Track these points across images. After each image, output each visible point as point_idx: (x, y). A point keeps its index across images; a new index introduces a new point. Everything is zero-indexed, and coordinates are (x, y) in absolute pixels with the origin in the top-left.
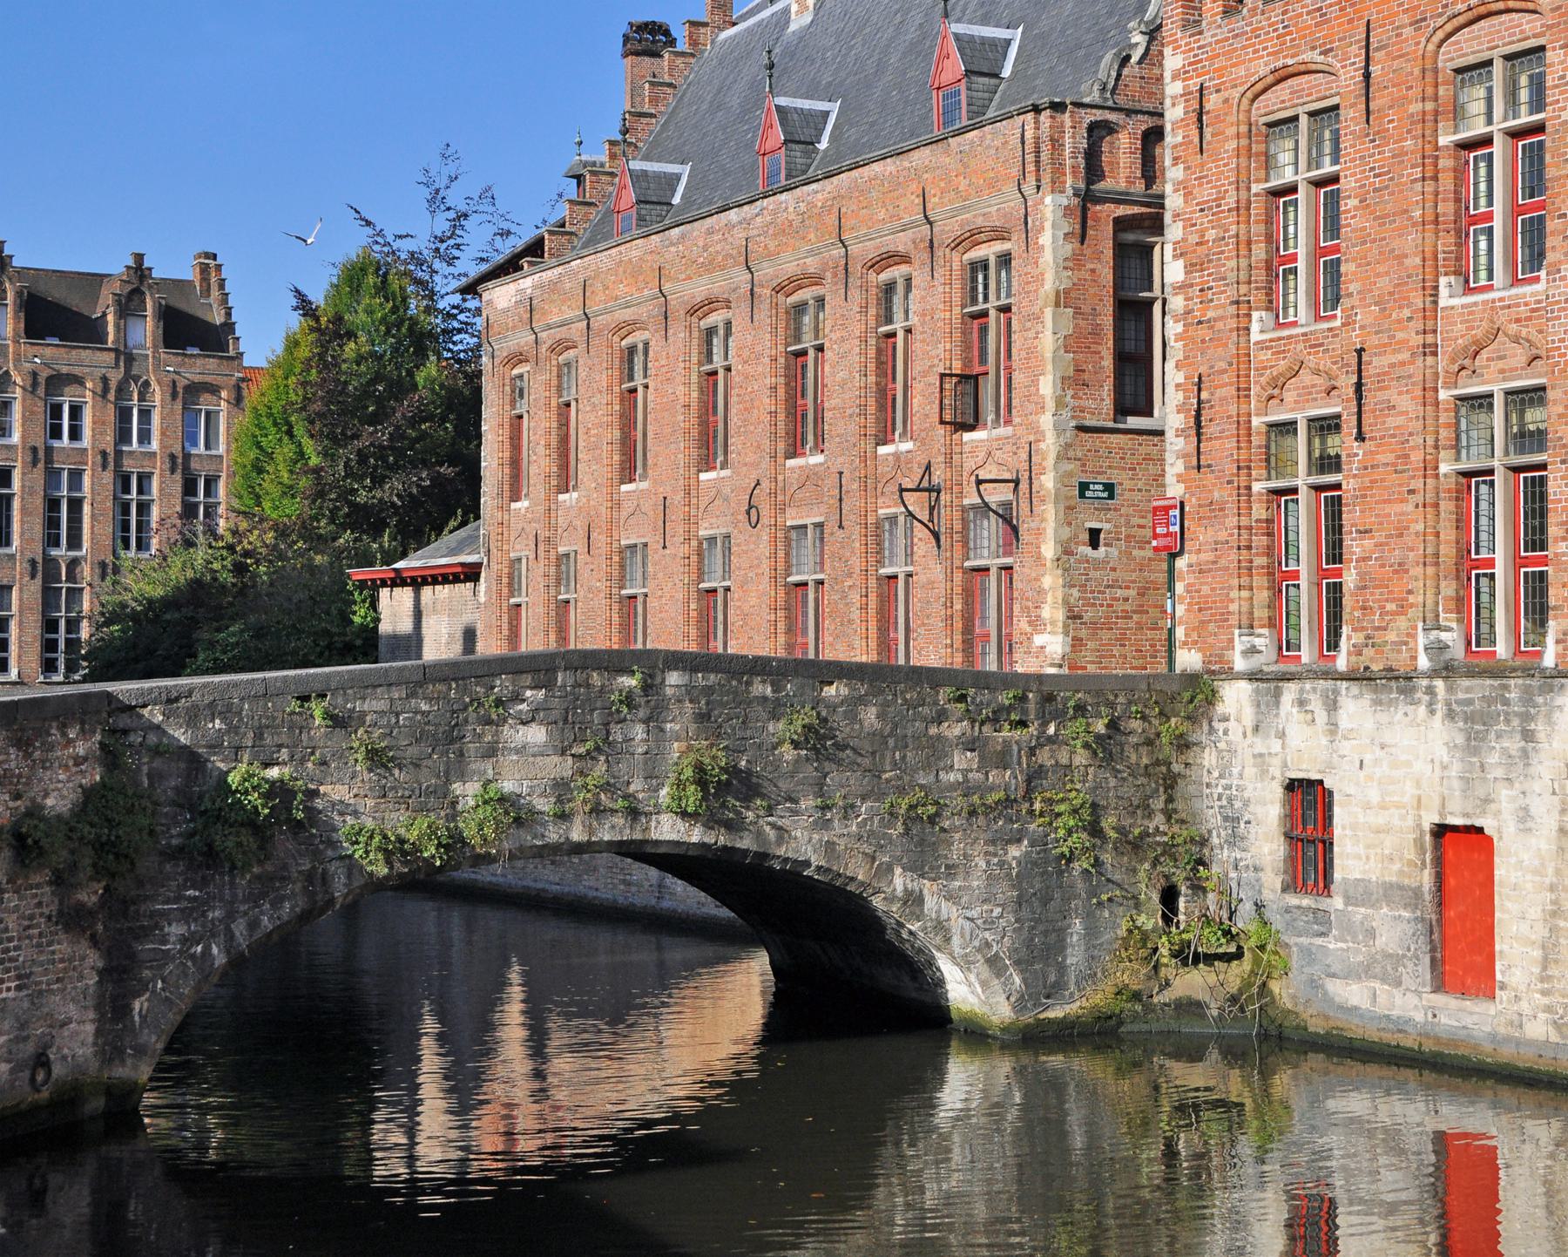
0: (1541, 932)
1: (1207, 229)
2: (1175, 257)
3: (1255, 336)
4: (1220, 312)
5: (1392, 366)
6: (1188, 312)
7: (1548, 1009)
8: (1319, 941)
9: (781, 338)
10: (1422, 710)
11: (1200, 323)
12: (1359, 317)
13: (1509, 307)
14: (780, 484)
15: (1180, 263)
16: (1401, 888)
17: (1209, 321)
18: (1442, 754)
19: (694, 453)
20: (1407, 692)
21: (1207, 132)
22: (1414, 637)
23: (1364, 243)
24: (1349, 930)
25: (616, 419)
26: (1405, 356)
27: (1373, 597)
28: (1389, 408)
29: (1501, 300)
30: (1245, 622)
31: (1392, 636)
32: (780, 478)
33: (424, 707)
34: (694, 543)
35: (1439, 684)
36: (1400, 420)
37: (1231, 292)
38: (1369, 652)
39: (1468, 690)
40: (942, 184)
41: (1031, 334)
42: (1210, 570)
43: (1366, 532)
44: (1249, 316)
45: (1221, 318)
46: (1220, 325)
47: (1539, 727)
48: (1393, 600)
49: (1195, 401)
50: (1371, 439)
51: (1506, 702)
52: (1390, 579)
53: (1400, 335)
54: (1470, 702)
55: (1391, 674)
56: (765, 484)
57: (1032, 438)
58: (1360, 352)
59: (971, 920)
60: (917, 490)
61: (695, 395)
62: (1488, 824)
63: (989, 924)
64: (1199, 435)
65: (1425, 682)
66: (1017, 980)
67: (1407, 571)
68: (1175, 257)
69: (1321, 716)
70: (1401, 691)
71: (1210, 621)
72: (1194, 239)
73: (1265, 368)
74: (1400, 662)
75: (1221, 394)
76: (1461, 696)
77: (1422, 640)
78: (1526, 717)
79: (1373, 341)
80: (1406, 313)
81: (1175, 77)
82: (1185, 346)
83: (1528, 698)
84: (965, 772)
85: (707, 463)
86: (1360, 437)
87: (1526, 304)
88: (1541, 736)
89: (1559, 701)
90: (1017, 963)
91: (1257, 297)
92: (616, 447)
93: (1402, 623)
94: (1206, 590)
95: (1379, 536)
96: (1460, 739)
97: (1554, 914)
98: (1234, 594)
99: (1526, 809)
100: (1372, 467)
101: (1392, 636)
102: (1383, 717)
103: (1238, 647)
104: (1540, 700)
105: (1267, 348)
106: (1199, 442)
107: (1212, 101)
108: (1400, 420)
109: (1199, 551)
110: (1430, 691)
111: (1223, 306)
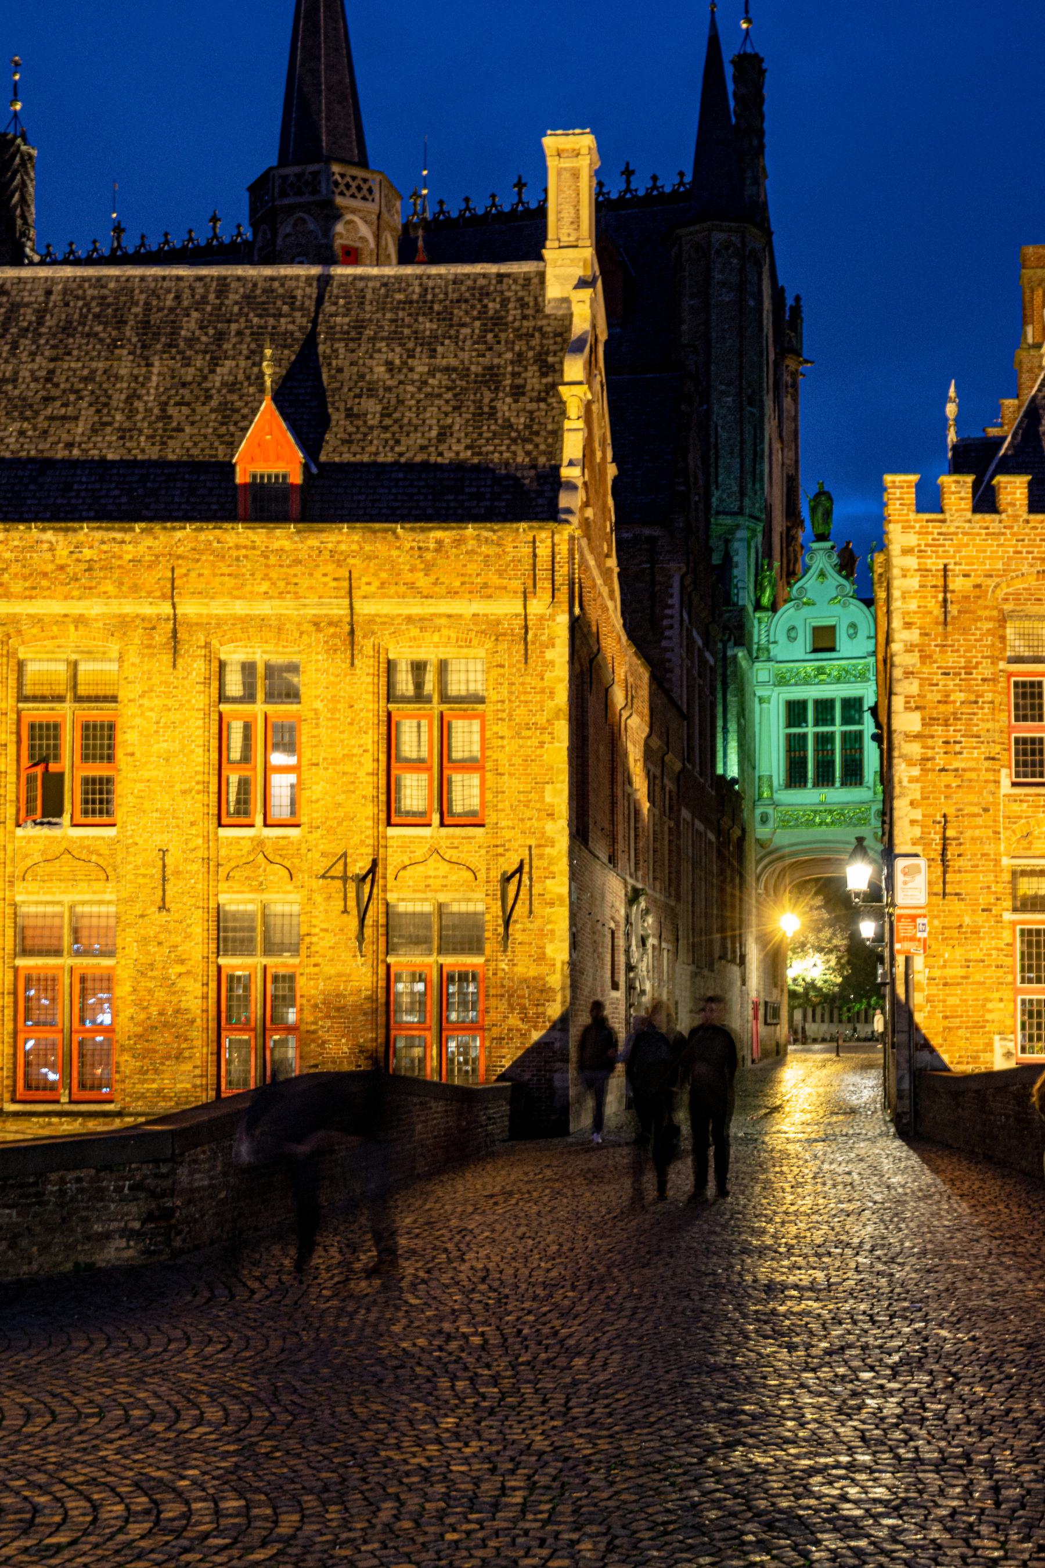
1: (953, 691)
4: (972, 764)
11: (943, 770)
14: (10, 853)
17: (956, 770)
32: (9, 847)
40: (384, 575)
42: (958, 984)
49: (938, 837)
57: (533, 842)
71: (959, 1028)
72: (933, 696)
73: (1020, 817)
82: (922, 788)
94: (951, 1001)
106: (945, 872)
107: (957, 584)
109: (944, 967)
111: (977, 759)
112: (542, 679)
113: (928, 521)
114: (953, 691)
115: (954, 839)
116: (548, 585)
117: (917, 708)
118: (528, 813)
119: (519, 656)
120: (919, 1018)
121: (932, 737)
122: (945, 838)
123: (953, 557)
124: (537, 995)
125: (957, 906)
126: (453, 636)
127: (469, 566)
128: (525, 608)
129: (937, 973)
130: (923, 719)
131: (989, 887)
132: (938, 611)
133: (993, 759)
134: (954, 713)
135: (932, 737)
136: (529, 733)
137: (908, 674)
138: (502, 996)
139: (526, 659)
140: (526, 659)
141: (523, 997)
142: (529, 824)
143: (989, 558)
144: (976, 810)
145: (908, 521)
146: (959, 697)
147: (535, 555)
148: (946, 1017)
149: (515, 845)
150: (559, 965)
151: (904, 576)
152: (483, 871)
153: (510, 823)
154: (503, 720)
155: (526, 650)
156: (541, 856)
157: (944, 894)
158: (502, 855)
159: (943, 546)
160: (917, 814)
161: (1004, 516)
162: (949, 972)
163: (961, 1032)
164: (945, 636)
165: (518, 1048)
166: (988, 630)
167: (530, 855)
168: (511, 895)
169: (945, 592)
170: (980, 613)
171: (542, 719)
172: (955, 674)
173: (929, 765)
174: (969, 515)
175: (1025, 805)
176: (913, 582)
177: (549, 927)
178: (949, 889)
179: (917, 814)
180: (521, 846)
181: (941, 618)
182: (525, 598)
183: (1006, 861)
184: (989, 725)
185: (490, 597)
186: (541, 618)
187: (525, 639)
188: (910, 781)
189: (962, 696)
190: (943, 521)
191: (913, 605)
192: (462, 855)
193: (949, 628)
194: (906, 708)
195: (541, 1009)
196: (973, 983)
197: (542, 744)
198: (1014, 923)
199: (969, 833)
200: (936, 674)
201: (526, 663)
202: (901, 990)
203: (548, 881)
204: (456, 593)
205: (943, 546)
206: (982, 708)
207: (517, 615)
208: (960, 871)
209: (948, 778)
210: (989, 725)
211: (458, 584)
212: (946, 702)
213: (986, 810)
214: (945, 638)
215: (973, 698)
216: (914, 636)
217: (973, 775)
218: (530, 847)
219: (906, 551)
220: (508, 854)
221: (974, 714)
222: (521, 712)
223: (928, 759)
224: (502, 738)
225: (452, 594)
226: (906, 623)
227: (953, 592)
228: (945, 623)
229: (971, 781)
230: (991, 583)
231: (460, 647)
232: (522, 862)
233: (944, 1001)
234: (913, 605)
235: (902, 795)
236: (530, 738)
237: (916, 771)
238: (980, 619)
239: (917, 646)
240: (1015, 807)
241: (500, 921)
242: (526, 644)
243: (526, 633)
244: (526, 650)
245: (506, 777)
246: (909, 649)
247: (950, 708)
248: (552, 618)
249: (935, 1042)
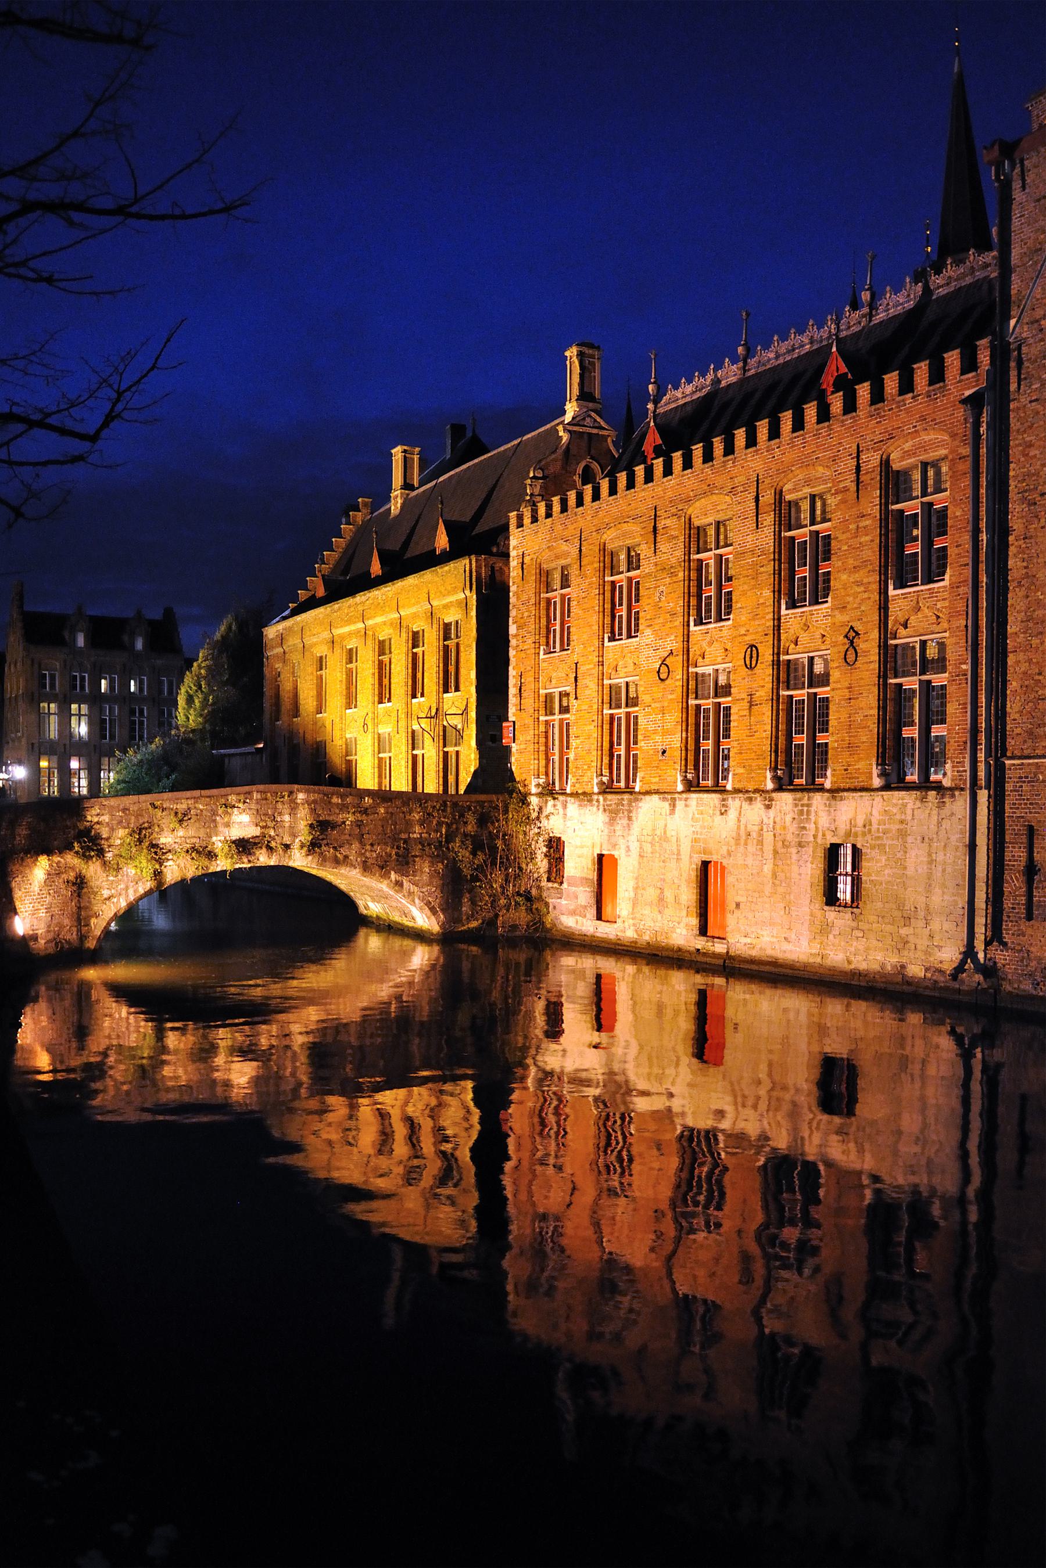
0: (632, 894)
2: (513, 623)
3: (542, 656)
5: (587, 669)
6: (518, 646)
7: (634, 925)
8: (559, 900)
9: (377, 653)
10: (595, 809)
15: (515, 626)
16: (586, 879)
18: (601, 825)
19: (344, 701)
20: (590, 801)
21: (525, 571)
22: (593, 779)
24: (568, 898)
25: (315, 686)
27: (580, 763)
30: (536, 773)
31: (585, 779)
33: (201, 807)
34: (344, 740)
35: (601, 798)
37: (532, 639)
38: (577, 785)
39: (610, 800)
41: (468, 653)
44: (539, 648)
46: (528, 652)
47: (633, 815)
51: (623, 805)
54: (610, 805)
55: (584, 794)
56: (370, 715)
58: (576, 664)
59: (423, 892)
60: (426, 718)
61: (344, 676)
62: (616, 853)
63: (430, 894)
64: (521, 696)
65: (595, 797)
66: (442, 916)
68: (513, 623)
69: (561, 811)
70: (588, 801)
74: (588, 790)
75: (528, 679)
76: (608, 803)
77: (595, 781)
78: (630, 811)
80: (593, 649)
81: (514, 548)
83: (630, 802)
84: (421, 834)
85: (349, 706)
86: (576, 698)
88: (634, 818)
89: (640, 804)
90: (442, 910)
91: (543, 640)
92: (315, 698)
95: (581, 739)
96: (607, 820)
97: (637, 888)
98: (532, 762)
99: (628, 847)
101: (585, 779)
102: (582, 811)
103: (533, 784)
104: (634, 804)
107: (527, 559)
110: (598, 801)
225: (449, 593)
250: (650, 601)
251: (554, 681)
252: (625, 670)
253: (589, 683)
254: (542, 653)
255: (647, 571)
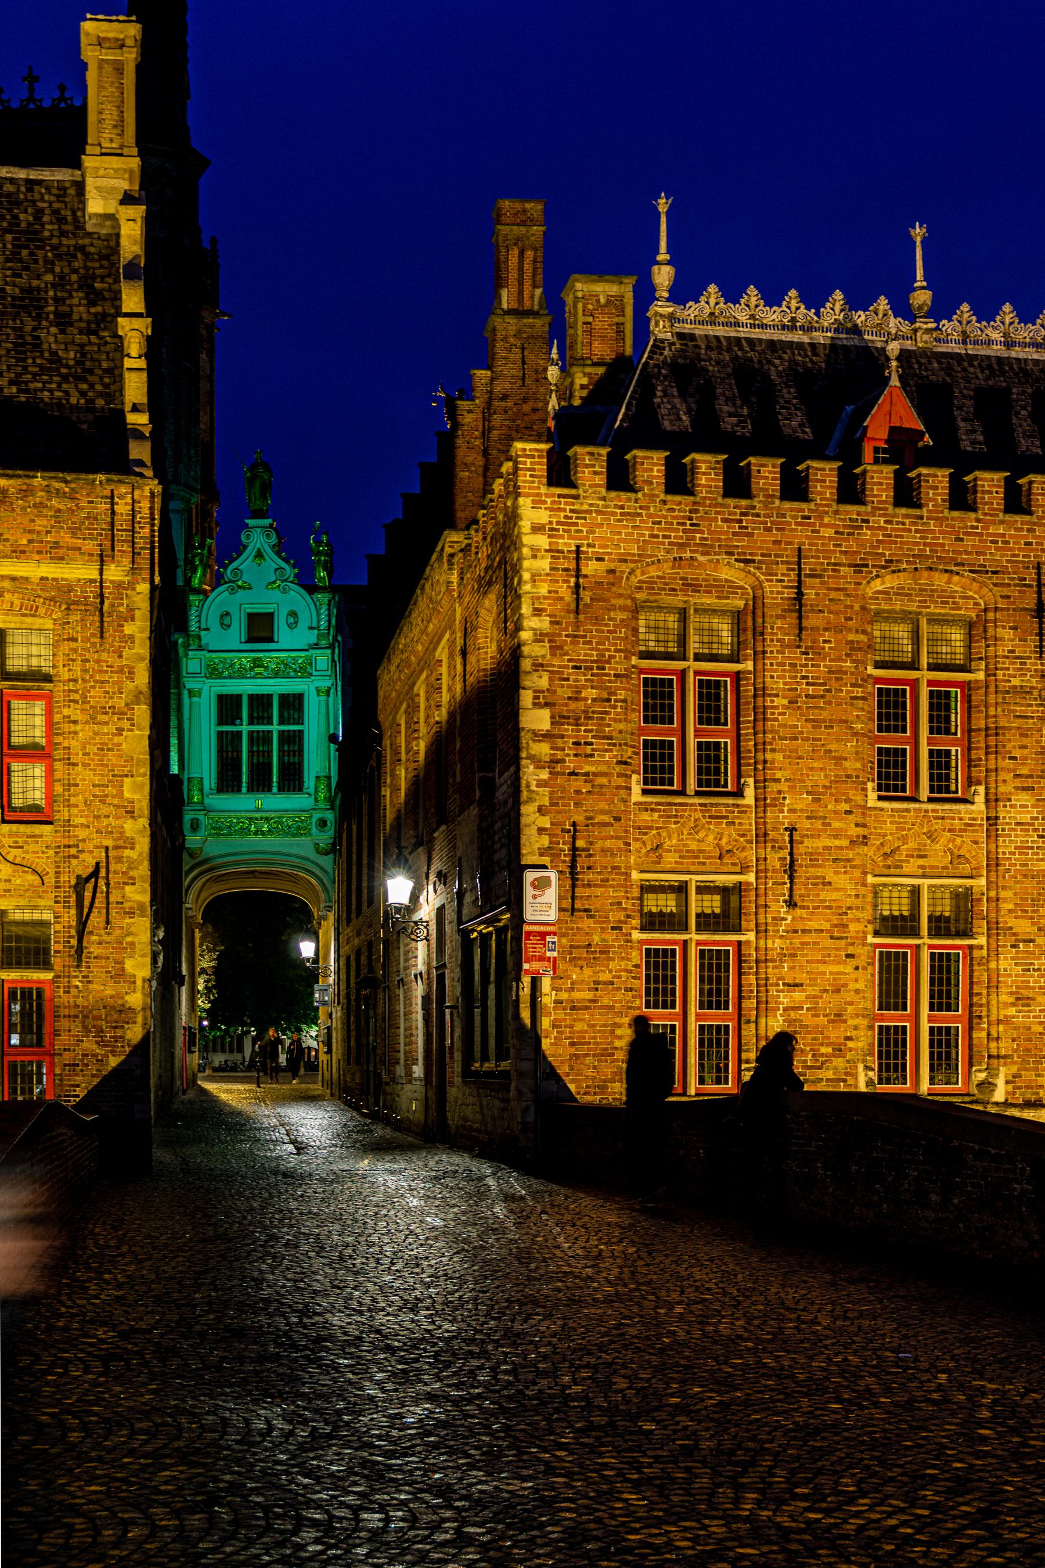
1: (584, 687)
4: (603, 768)
5: (829, 848)
12: (787, 802)
13: (943, 818)
15: (545, 714)
17: (587, 774)
23: (796, 739)
26: (845, 843)
28: (824, 884)
29: (933, 811)
36: (835, 895)
42: (586, 1008)
43: (796, 985)
45: (605, 774)
48: (828, 1045)
50: (803, 907)
52: (823, 1027)
53: (836, 825)
57: (109, 843)
67: (845, 1021)
71: (587, 1055)
72: (565, 692)
73: (651, 828)
79: (803, 824)
82: (551, 793)
87: (961, 819)
93: (839, 1063)
94: (579, 1026)
100: (803, 931)
105: (652, 810)
106: (573, 886)
107: (590, 568)
108: (835, 895)
112: (120, 657)
113: (560, 496)
114: (584, 687)
115: (584, 850)
116: (127, 547)
117: (547, 704)
118: (105, 810)
119: (94, 629)
120: (546, 1044)
121: (562, 737)
122: (574, 849)
123: (587, 538)
124: (115, 1016)
125: (587, 923)
126: (17, 603)
127: (38, 522)
128: (101, 574)
129: (564, 996)
130: (552, 717)
131: (620, 903)
132: (569, 597)
133: (626, 763)
134: (585, 712)
135: (562, 737)
136: (105, 718)
137: (538, 666)
138: (76, 1016)
139: (102, 632)
140: (102, 632)
141: (100, 1018)
142: (106, 822)
143: (624, 541)
144: (606, 818)
145: (538, 495)
146: (590, 693)
147: (113, 513)
148: (572, 1044)
149: (90, 845)
150: (139, 983)
151: (535, 557)
152: (52, 874)
153: (84, 821)
154: (76, 702)
155: (102, 622)
156: (119, 859)
157: (573, 910)
158: (75, 857)
159: (576, 524)
160: (545, 822)
161: (640, 495)
162: (577, 995)
163: (588, 1061)
164: (577, 625)
165: (94, 1076)
166: (622, 620)
167: (107, 857)
168: (87, 903)
169: (577, 576)
170: (614, 601)
171: (120, 703)
172: (586, 668)
173: (558, 768)
174: (603, 491)
175: (656, 814)
176: (544, 564)
177: (129, 939)
178: (578, 905)
179: (545, 822)
180: (98, 847)
181: (573, 606)
182: (102, 561)
183: (635, 875)
184: (621, 726)
185: (62, 559)
186: (119, 586)
187: (101, 610)
188: (538, 786)
189: (594, 693)
190: (576, 497)
191: (543, 589)
192: (27, 856)
193: (581, 617)
194: (534, 704)
195: (119, 1032)
196: (601, 1007)
197: (120, 731)
198: (642, 942)
199: (599, 844)
200: (567, 667)
201: (102, 637)
202: (525, 1015)
203: (127, 888)
204: (23, 552)
205: (576, 524)
206: (615, 707)
207: (92, 581)
208: (589, 886)
209: (578, 783)
210: (621, 726)
211: (24, 542)
212: (576, 699)
213: (617, 819)
214: (577, 629)
215: (606, 696)
216: (543, 623)
217: (604, 780)
218: (107, 848)
219: (537, 529)
220: (82, 856)
221: (606, 713)
222: (97, 692)
223: (557, 762)
224: (75, 722)
226: (535, 609)
227: (586, 576)
228: (577, 612)
229: (601, 786)
230: (626, 568)
231: (24, 615)
232: (98, 864)
233: (572, 1026)
234: (543, 589)
235: (530, 800)
236: (106, 723)
237: (544, 775)
238: (613, 608)
239: (547, 635)
240: (646, 816)
241: (73, 932)
242: (102, 615)
243: (102, 603)
244: (102, 622)
245: (80, 768)
246: (539, 637)
247: (581, 706)
248: (131, 586)
249: (562, 1070)
250: (1025, 741)
251: (670, 859)
252: (921, 862)
253: (830, 877)
254: (636, 789)
255: (1016, 682)
